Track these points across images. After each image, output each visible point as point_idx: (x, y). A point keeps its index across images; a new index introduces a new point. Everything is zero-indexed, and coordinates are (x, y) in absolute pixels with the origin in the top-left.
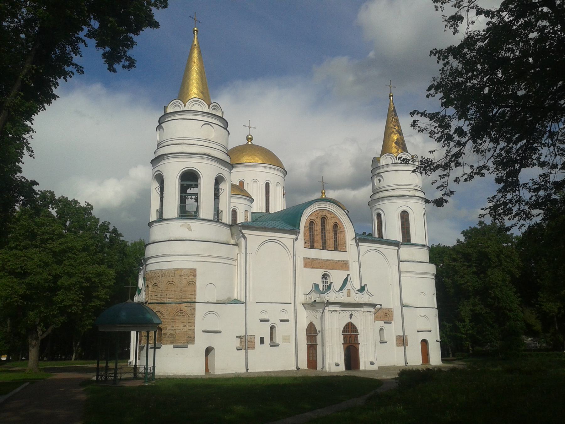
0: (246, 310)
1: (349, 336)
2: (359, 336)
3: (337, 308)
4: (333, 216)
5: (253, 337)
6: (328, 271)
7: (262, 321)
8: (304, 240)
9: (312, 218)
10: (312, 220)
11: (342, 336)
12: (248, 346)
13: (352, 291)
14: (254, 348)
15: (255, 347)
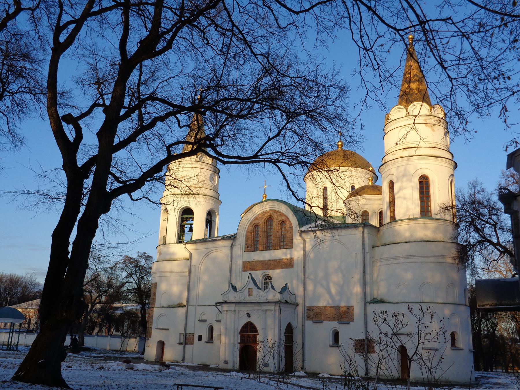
0: (187, 312)
1: (246, 335)
2: (258, 336)
3: (232, 307)
4: (279, 214)
5: (192, 336)
6: (268, 271)
7: (201, 321)
8: (246, 244)
9: (256, 222)
10: (255, 225)
11: (239, 336)
12: (187, 342)
13: (253, 289)
14: (192, 344)
15: (193, 343)
